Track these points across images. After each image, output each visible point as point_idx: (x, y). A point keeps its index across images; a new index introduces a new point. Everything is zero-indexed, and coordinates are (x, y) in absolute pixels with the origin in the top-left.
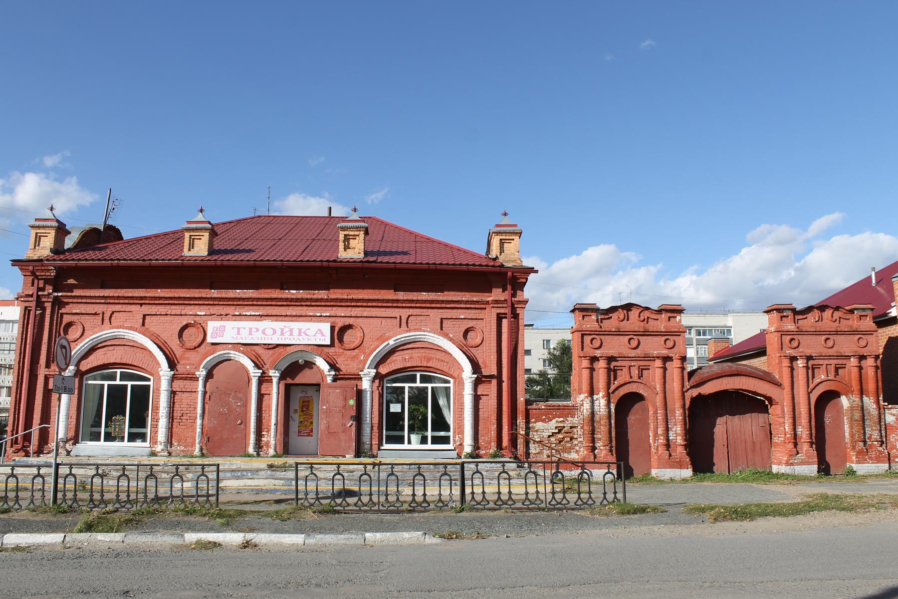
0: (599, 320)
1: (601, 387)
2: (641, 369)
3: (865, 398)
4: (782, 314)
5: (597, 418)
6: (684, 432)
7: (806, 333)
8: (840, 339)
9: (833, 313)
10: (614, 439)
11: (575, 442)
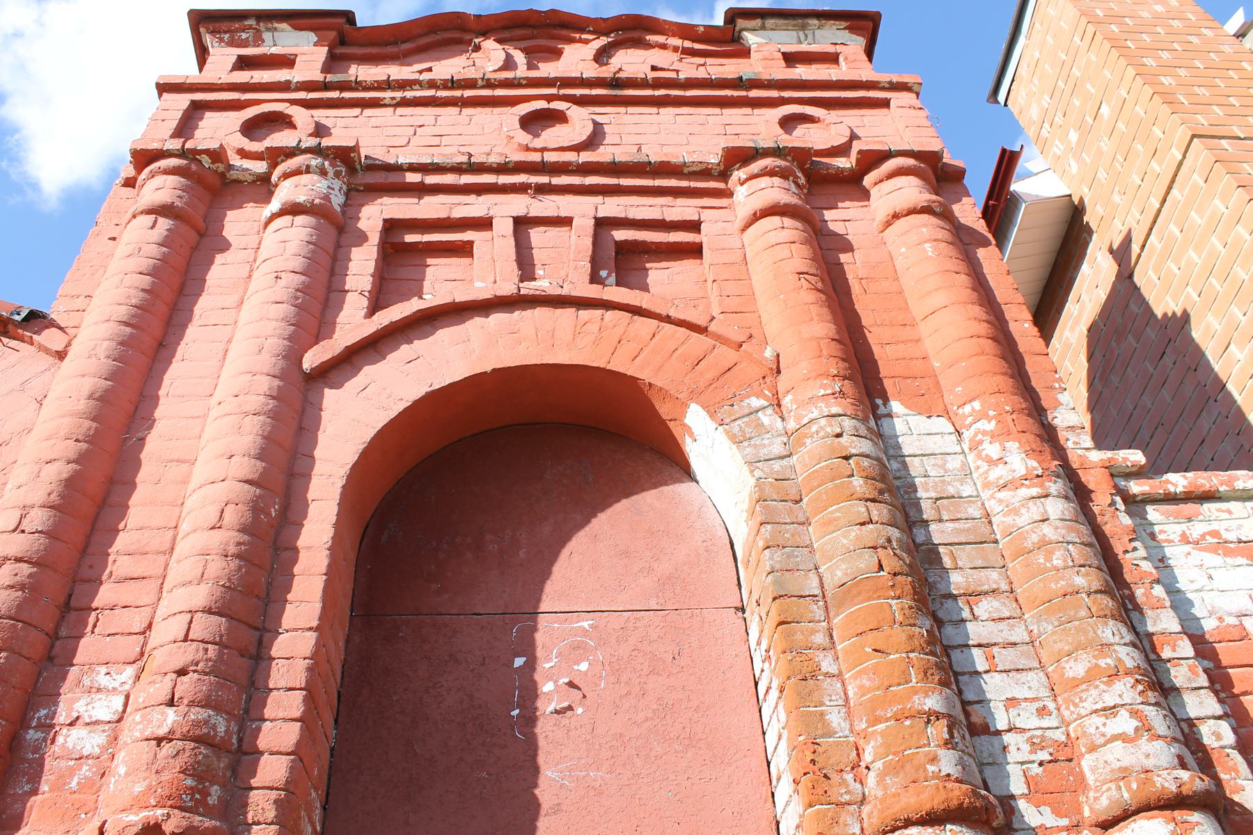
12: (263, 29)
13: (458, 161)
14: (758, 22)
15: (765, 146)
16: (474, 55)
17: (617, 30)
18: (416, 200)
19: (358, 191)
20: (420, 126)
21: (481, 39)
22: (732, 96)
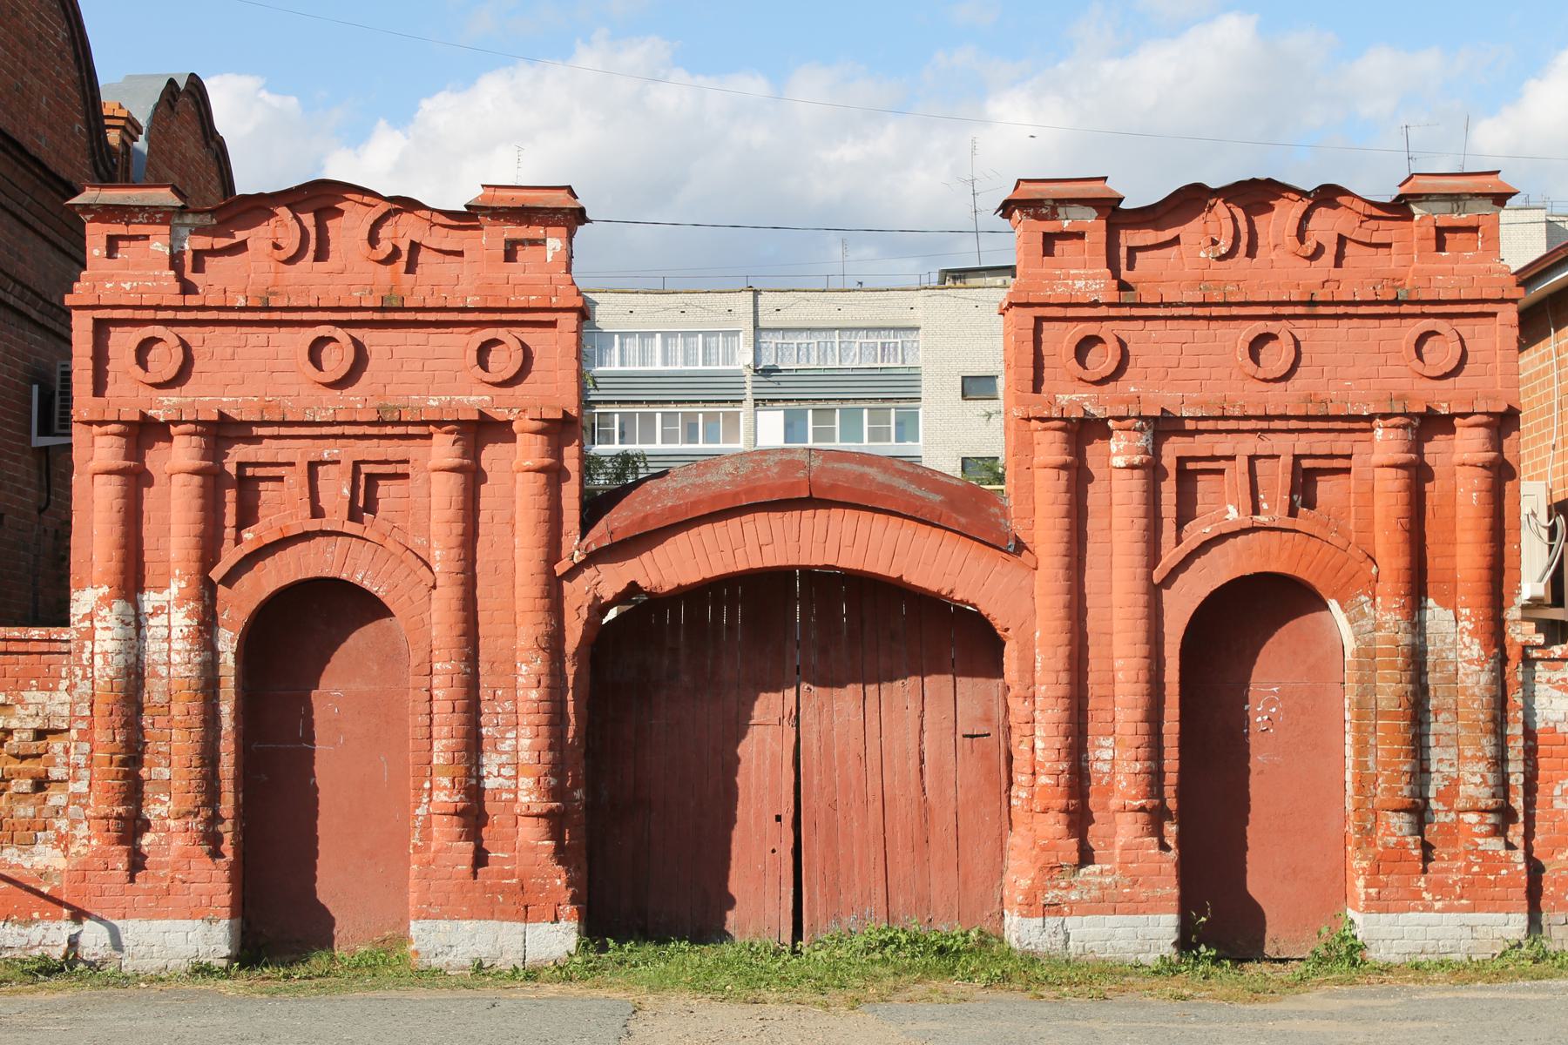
0: (188, 258)
1: (174, 554)
2: (369, 476)
3: (1437, 616)
4: (1050, 226)
5: (154, 691)
6: (547, 756)
7: (1161, 312)
8: (1320, 337)
9: (1306, 217)
10: (227, 787)
11: (56, 798)
21: (1214, 200)
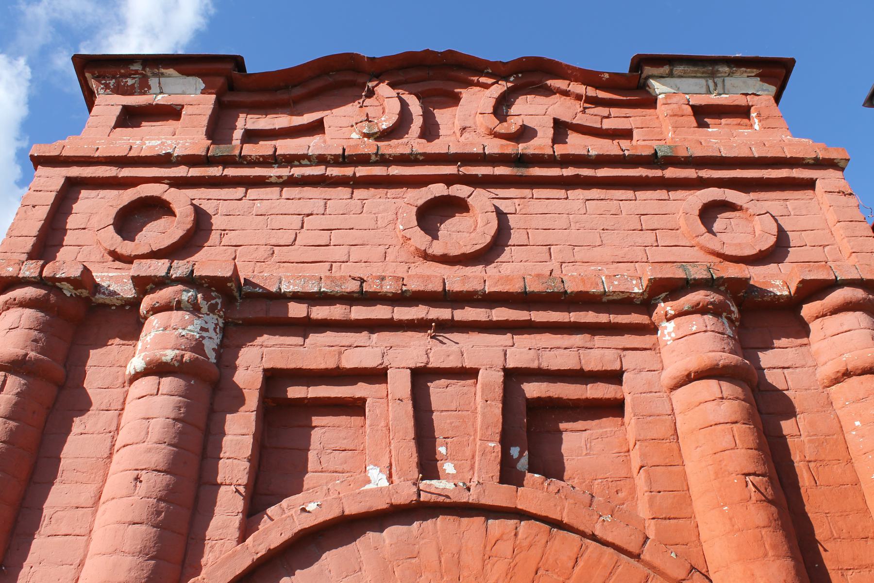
12: (149, 74)
13: (348, 290)
14: (666, 69)
15: (698, 276)
16: (368, 102)
17: (517, 73)
18: (299, 340)
19: (236, 325)
20: (308, 215)
21: (375, 83)
22: (647, 176)
